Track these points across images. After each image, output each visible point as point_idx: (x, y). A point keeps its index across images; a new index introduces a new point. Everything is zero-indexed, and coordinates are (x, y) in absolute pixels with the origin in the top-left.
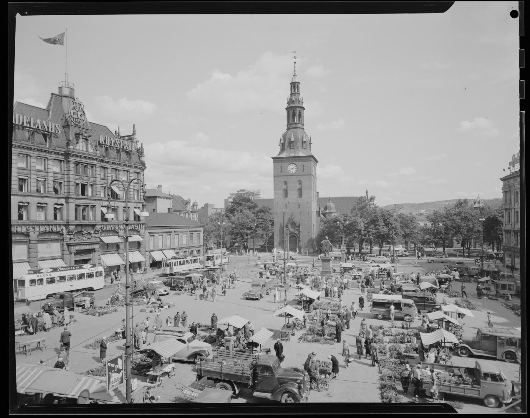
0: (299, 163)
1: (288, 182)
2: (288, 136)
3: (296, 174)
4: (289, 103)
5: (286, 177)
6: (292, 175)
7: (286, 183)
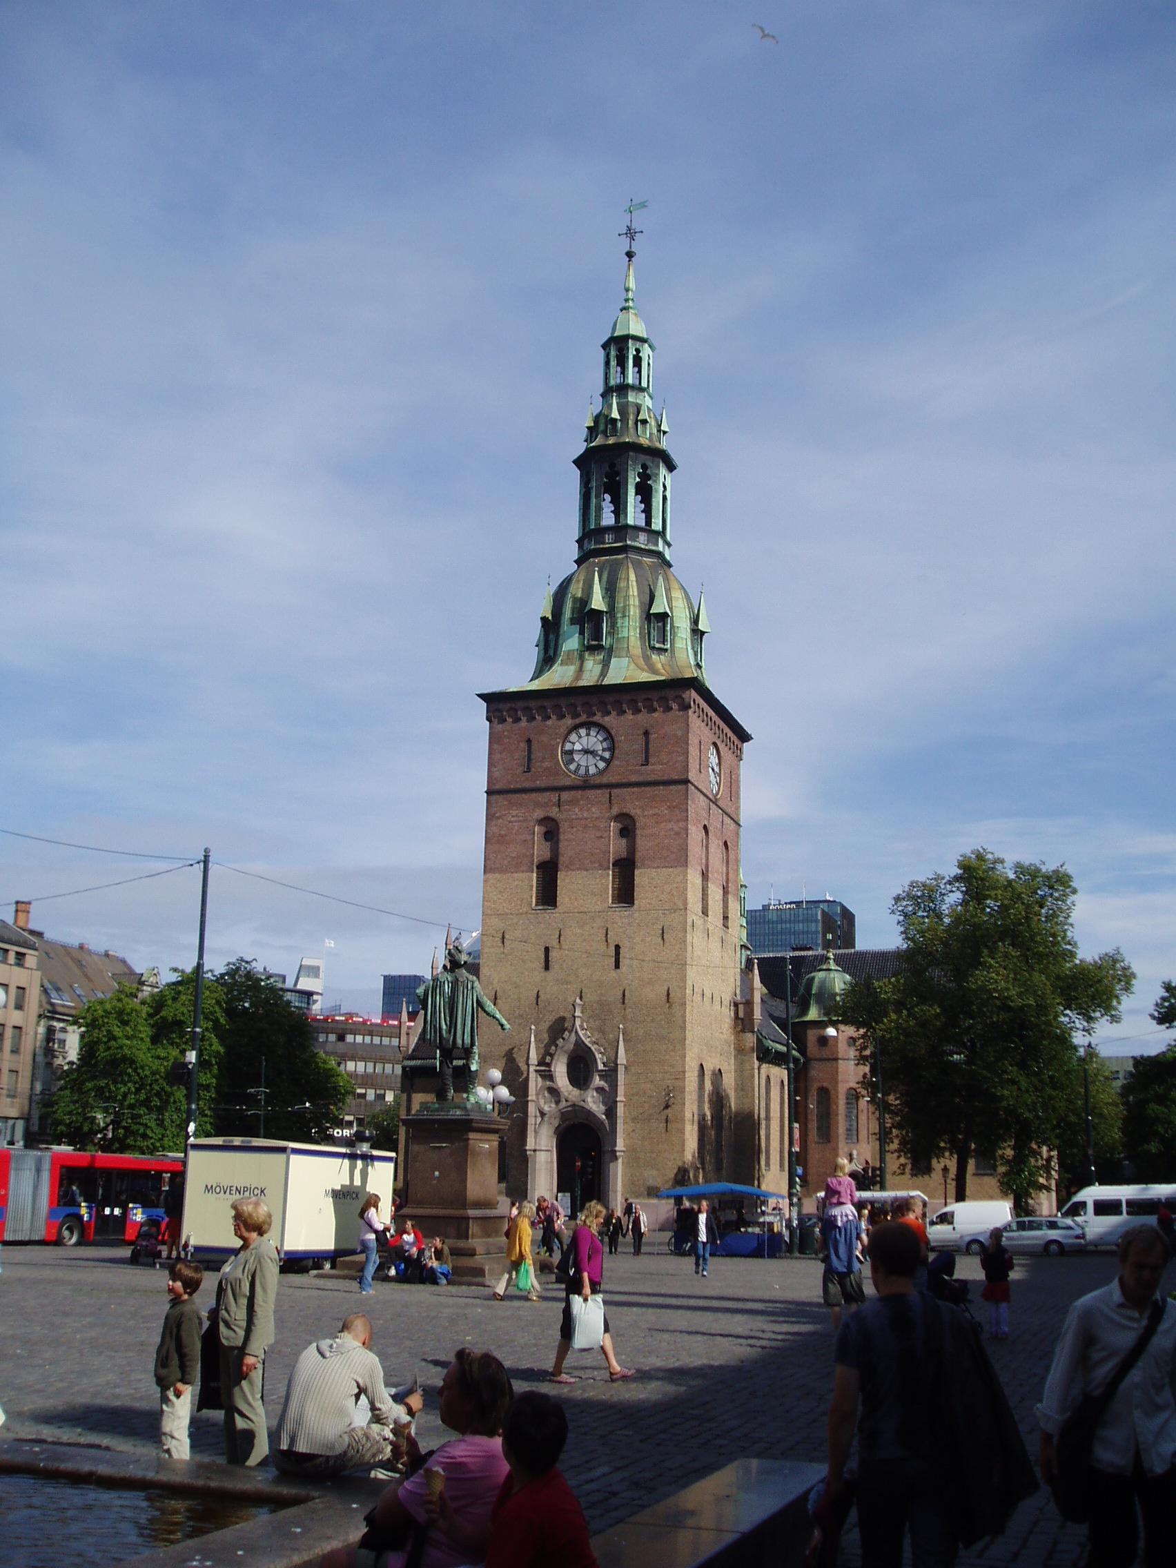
0: (624, 723)
1: (564, 827)
2: (576, 590)
3: (605, 780)
4: (592, 431)
5: (554, 797)
6: (586, 785)
7: (552, 832)
